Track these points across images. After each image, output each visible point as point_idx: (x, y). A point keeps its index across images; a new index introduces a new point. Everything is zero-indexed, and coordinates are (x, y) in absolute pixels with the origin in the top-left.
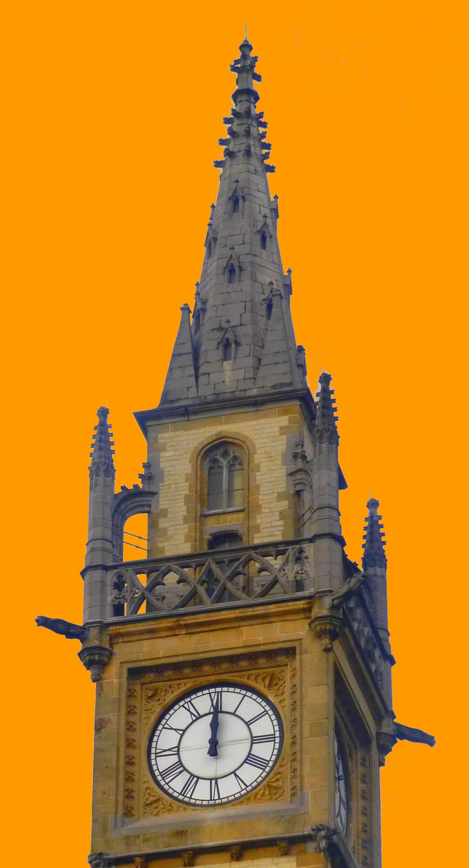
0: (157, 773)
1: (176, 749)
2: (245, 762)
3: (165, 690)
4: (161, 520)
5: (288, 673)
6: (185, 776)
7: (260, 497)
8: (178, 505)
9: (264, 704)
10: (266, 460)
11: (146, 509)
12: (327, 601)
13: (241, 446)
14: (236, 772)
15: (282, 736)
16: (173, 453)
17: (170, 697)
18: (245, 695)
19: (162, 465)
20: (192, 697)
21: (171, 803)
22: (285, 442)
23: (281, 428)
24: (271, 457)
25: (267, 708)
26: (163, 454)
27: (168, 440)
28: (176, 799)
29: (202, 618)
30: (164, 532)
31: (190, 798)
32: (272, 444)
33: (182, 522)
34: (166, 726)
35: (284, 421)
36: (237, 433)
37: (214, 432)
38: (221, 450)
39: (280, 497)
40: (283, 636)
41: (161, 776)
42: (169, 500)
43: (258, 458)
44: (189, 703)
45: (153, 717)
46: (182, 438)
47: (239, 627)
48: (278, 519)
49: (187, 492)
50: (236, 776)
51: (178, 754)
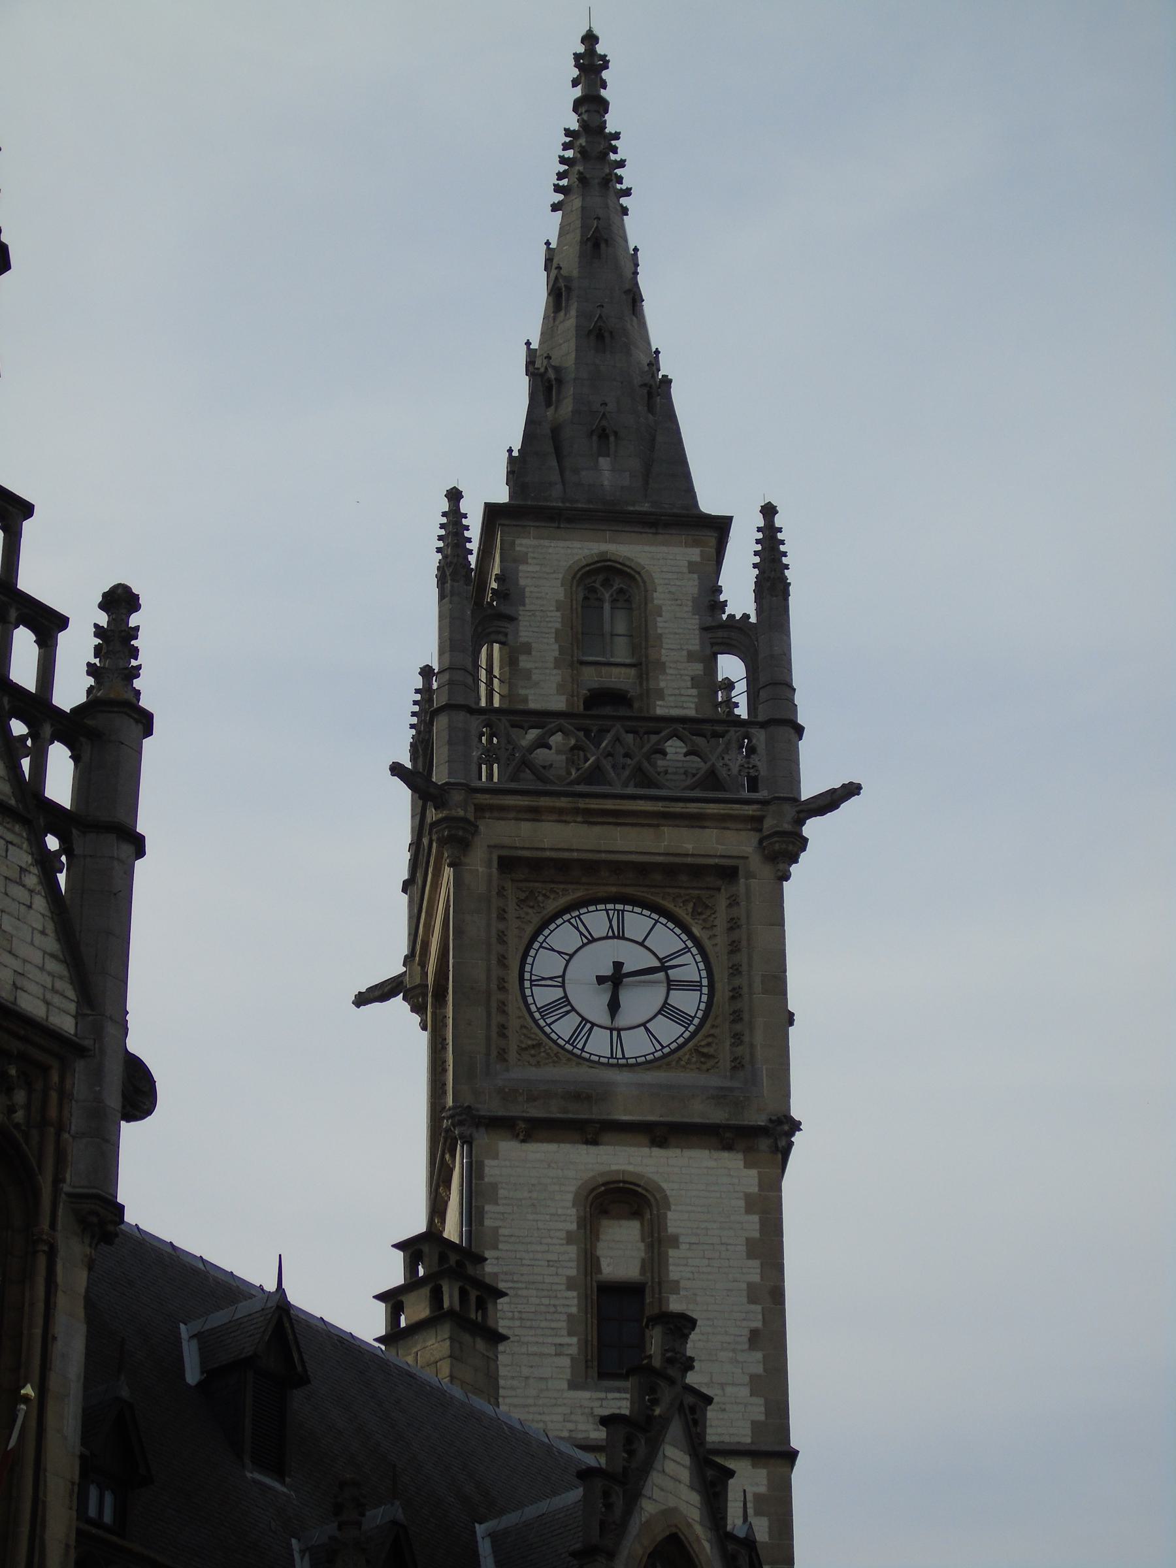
0: (533, 1008)
1: (560, 979)
2: (659, 1013)
3: (544, 895)
4: (522, 658)
5: (722, 902)
6: (572, 1021)
7: (663, 651)
8: (545, 640)
9: (684, 937)
10: (670, 602)
11: (503, 639)
12: (790, 811)
13: (633, 578)
14: (648, 1025)
15: (711, 986)
16: (537, 568)
17: (552, 906)
18: (657, 921)
19: (522, 582)
20: (582, 911)
21: (558, 1053)
22: (696, 583)
23: (690, 563)
24: (677, 600)
25: (689, 944)
26: (521, 567)
27: (530, 550)
28: (562, 1048)
29: (609, 805)
30: (528, 674)
31: (582, 1050)
32: (678, 583)
33: (552, 665)
34: (545, 945)
35: (694, 554)
36: (629, 559)
37: (596, 551)
38: (601, 577)
39: (691, 657)
40: (721, 849)
41: (540, 1013)
42: (534, 632)
43: (659, 597)
44: (577, 918)
45: (529, 930)
46: (550, 550)
47: (658, 826)
48: (690, 686)
49: (558, 626)
50: (647, 1030)
51: (563, 986)
